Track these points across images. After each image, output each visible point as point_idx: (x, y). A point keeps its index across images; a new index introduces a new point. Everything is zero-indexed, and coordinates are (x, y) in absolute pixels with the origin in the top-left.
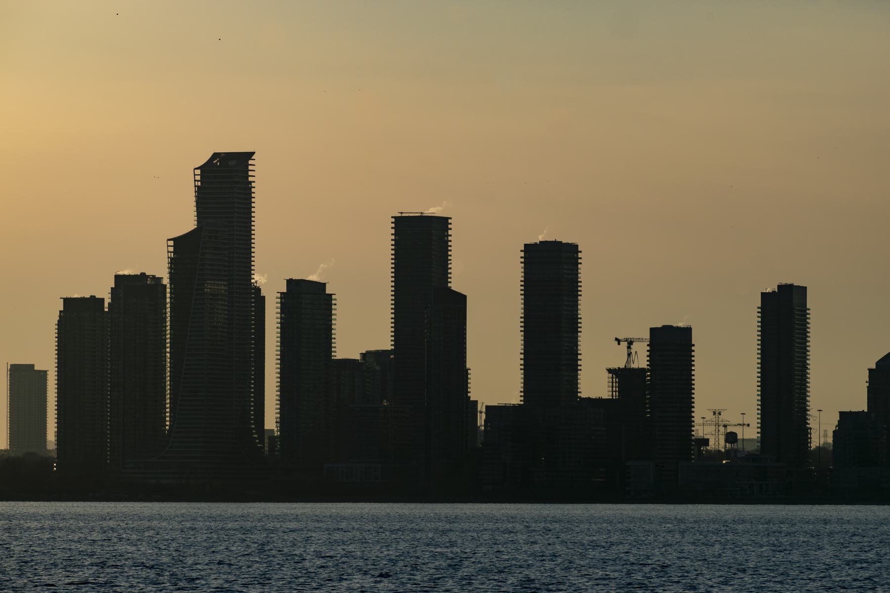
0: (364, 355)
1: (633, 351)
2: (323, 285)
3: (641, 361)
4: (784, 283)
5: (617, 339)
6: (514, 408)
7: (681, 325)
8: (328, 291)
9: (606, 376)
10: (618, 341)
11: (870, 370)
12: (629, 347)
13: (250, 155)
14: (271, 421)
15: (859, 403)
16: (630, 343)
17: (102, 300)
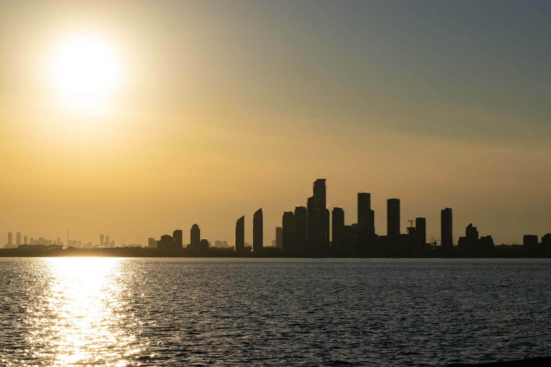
0: (352, 225)
1: (412, 223)
2: (342, 209)
3: (414, 225)
4: (446, 208)
6: (385, 236)
7: (423, 217)
8: (343, 210)
9: (406, 229)
10: (409, 221)
11: (467, 228)
12: (411, 222)
14: (331, 240)
15: (464, 235)
16: (412, 222)
17: (293, 212)
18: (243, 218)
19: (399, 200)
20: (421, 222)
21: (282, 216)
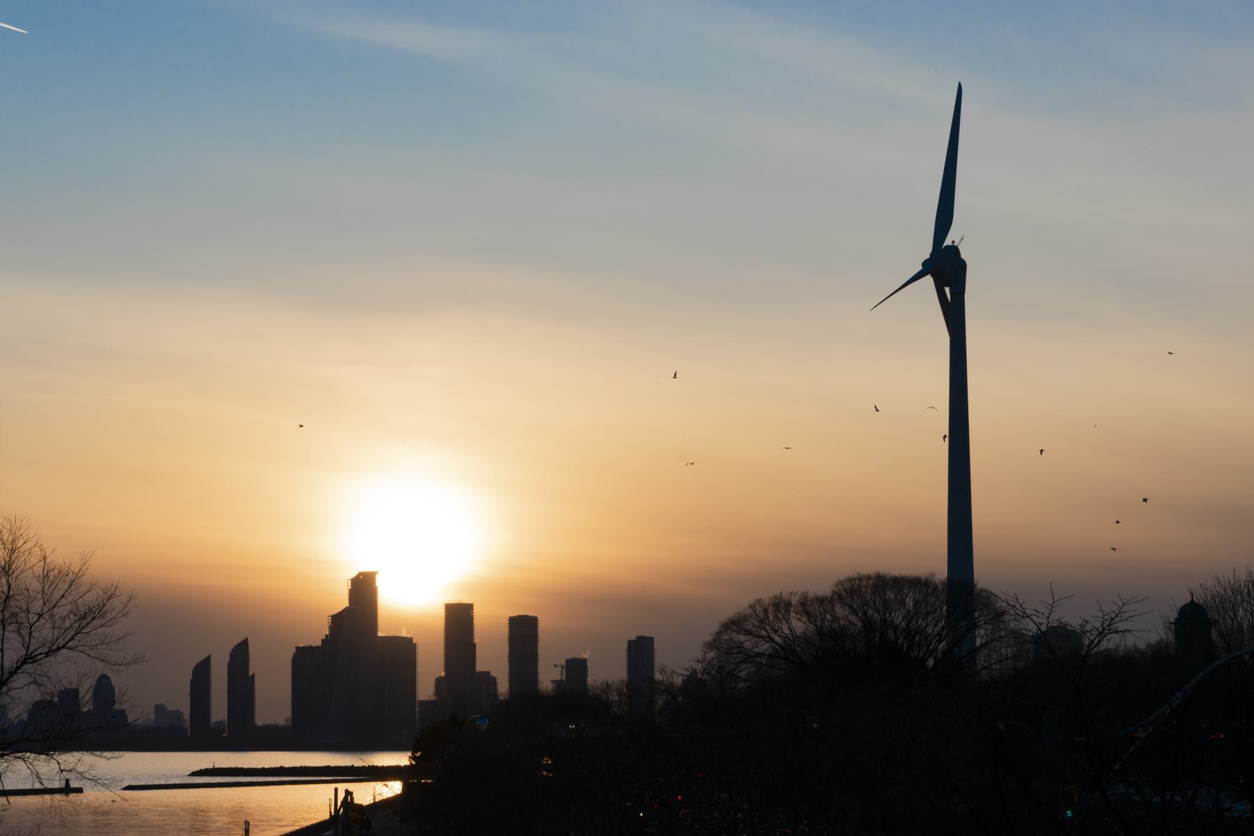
5: (555, 665)
8: (414, 641)
9: (550, 682)
10: (556, 666)
13: (376, 573)
18: (208, 660)
19: (537, 618)
20: (576, 667)
21: (292, 656)
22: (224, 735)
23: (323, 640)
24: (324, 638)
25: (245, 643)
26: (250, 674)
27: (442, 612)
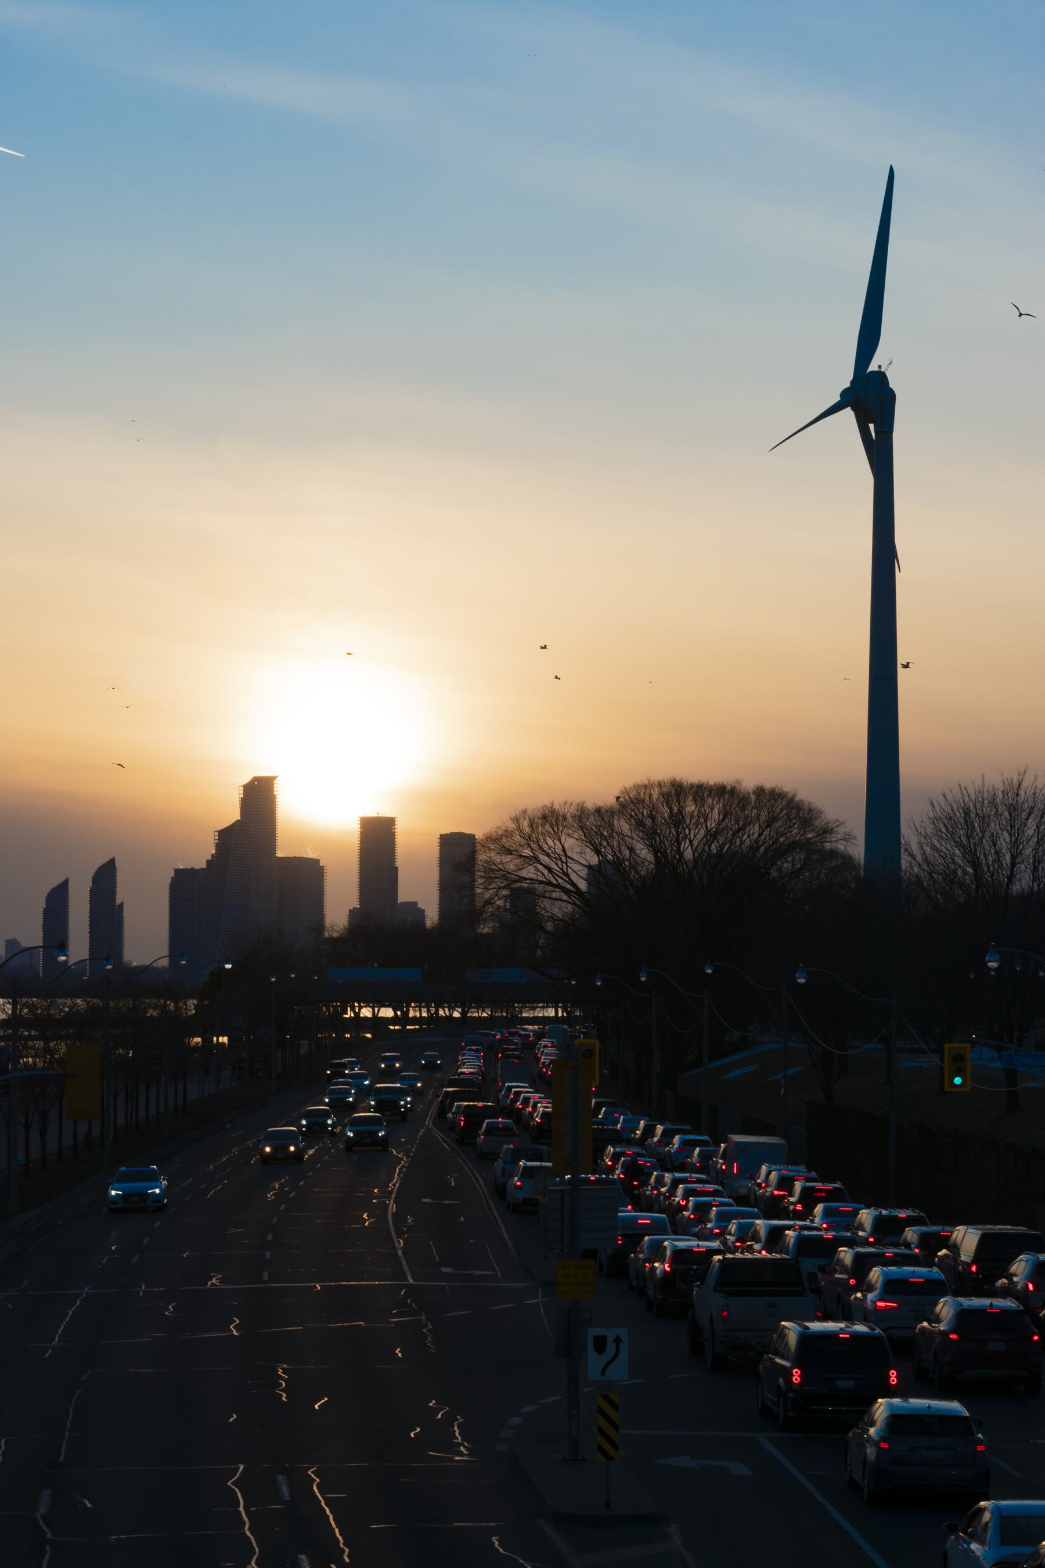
2: (318, 861)
8: (321, 864)
13: (274, 778)
18: (64, 886)
21: (169, 881)
22: (85, 978)
23: (208, 862)
24: (210, 858)
25: (111, 864)
26: (118, 902)
27: (355, 827)
